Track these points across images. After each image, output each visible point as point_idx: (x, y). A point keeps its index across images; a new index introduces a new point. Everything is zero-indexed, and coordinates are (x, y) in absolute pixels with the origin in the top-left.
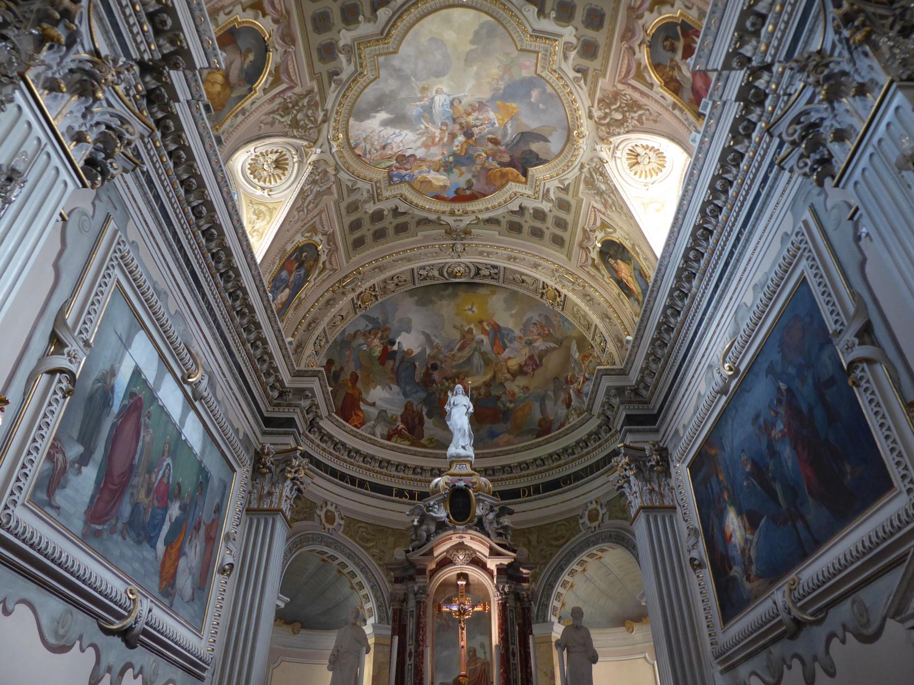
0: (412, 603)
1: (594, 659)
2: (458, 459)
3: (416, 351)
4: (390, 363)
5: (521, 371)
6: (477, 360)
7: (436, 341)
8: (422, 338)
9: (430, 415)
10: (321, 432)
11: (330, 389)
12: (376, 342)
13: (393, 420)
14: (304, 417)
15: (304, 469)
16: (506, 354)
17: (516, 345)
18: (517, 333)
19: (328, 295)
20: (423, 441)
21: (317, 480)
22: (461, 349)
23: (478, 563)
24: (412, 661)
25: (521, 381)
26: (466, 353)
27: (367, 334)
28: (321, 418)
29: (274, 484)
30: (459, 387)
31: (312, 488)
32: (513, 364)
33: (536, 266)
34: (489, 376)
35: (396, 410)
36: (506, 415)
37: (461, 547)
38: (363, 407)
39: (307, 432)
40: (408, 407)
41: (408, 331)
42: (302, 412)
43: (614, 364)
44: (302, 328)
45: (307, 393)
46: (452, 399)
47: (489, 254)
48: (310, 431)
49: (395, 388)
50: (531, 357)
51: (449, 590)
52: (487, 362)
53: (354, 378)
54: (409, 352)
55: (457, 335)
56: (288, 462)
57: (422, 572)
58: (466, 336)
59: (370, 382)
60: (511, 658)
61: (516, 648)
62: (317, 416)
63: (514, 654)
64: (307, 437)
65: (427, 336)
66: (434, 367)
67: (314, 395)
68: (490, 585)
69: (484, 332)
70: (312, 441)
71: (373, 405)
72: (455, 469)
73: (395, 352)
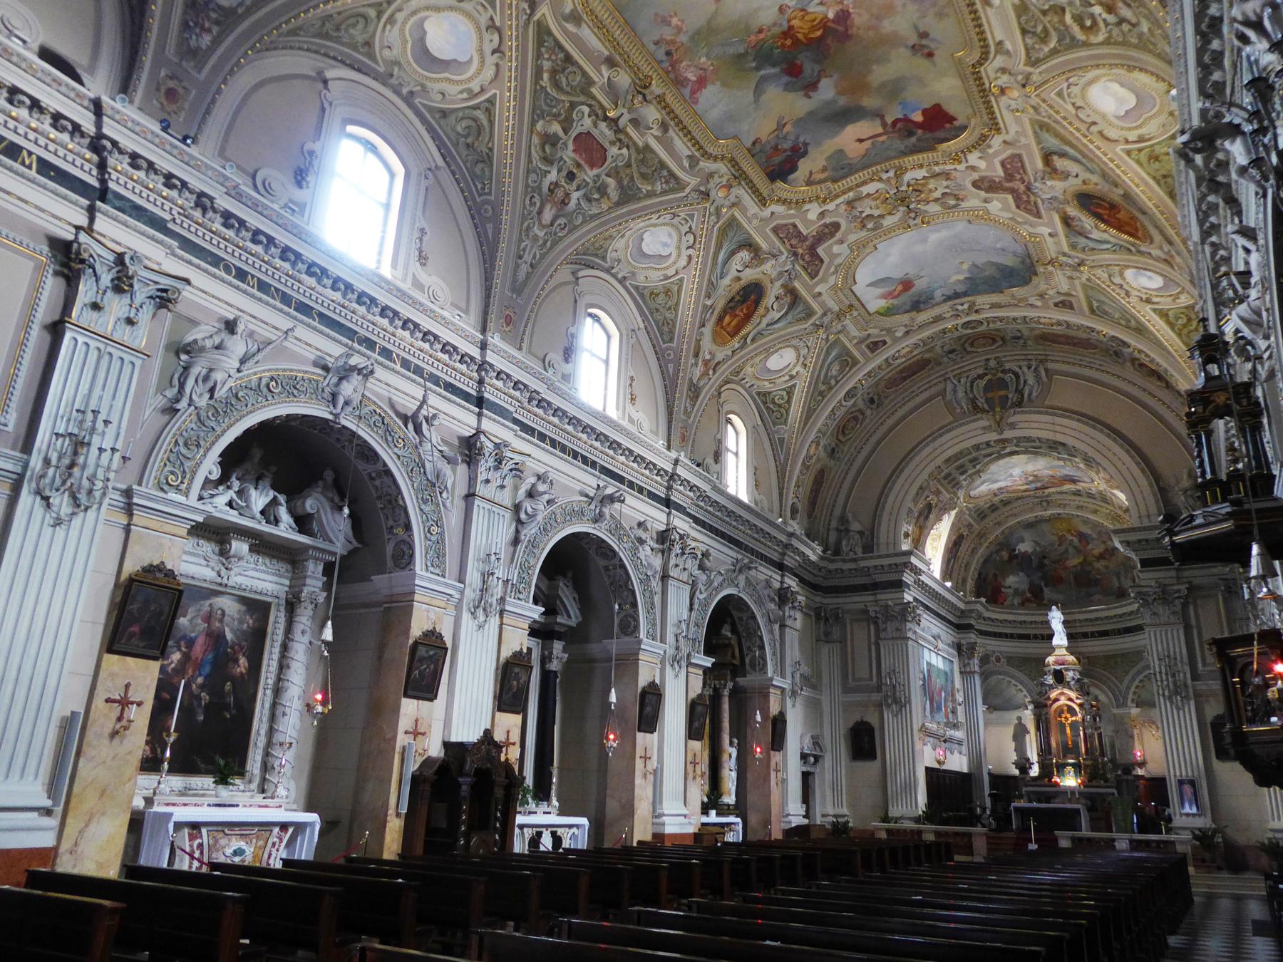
2: (1060, 647)
3: (1030, 550)
4: (1015, 561)
5: (1101, 557)
6: (1071, 550)
7: (1043, 543)
8: (1033, 544)
9: (1046, 586)
12: (1004, 553)
13: (1023, 593)
16: (1090, 547)
17: (1096, 542)
18: (1095, 536)
19: (973, 546)
22: (1060, 545)
23: (1070, 699)
25: (1103, 563)
26: (1063, 548)
27: (997, 552)
29: (970, 659)
30: (1054, 607)
32: (1096, 552)
33: (1096, 512)
35: (1024, 587)
36: (1096, 582)
37: (1062, 694)
38: (1003, 590)
40: (1032, 584)
41: (1023, 541)
44: (963, 570)
47: (1065, 505)
49: (1021, 574)
50: (1107, 549)
51: (1060, 712)
52: (1079, 551)
53: (995, 575)
54: (1026, 552)
55: (1056, 538)
56: (974, 649)
57: (1046, 706)
58: (1062, 539)
59: (1005, 576)
65: (1037, 543)
68: (1077, 709)
69: (1072, 535)
71: (1010, 587)
72: (1057, 652)
73: (1017, 555)
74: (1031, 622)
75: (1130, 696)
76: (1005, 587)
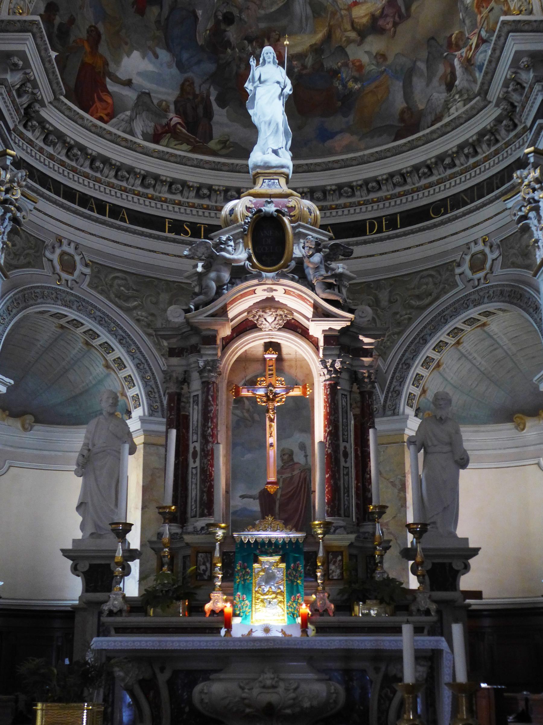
0: (196, 385)
1: (463, 463)
9: (222, 103)
10: (43, 128)
11: (54, 54)
14: (14, 102)
15: (20, 186)
20: (212, 145)
21: (42, 204)
24: (198, 464)
28: (43, 105)
30: (268, 51)
31: (35, 217)
34: (319, 36)
38: (112, 87)
39: (21, 128)
42: (9, 92)
43: (531, 12)
45: (16, 60)
46: (256, 71)
48: (25, 126)
49: (164, 55)
57: (211, 340)
60: (342, 459)
61: (351, 446)
62: (36, 100)
63: (346, 455)
64: (22, 136)
66: (229, 19)
67: (27, 65)
70: (30, 143)
71: (128, 83)
72: (262, 187)
74: (171, 184)
75: (409, 388)
76: (117, 80)
